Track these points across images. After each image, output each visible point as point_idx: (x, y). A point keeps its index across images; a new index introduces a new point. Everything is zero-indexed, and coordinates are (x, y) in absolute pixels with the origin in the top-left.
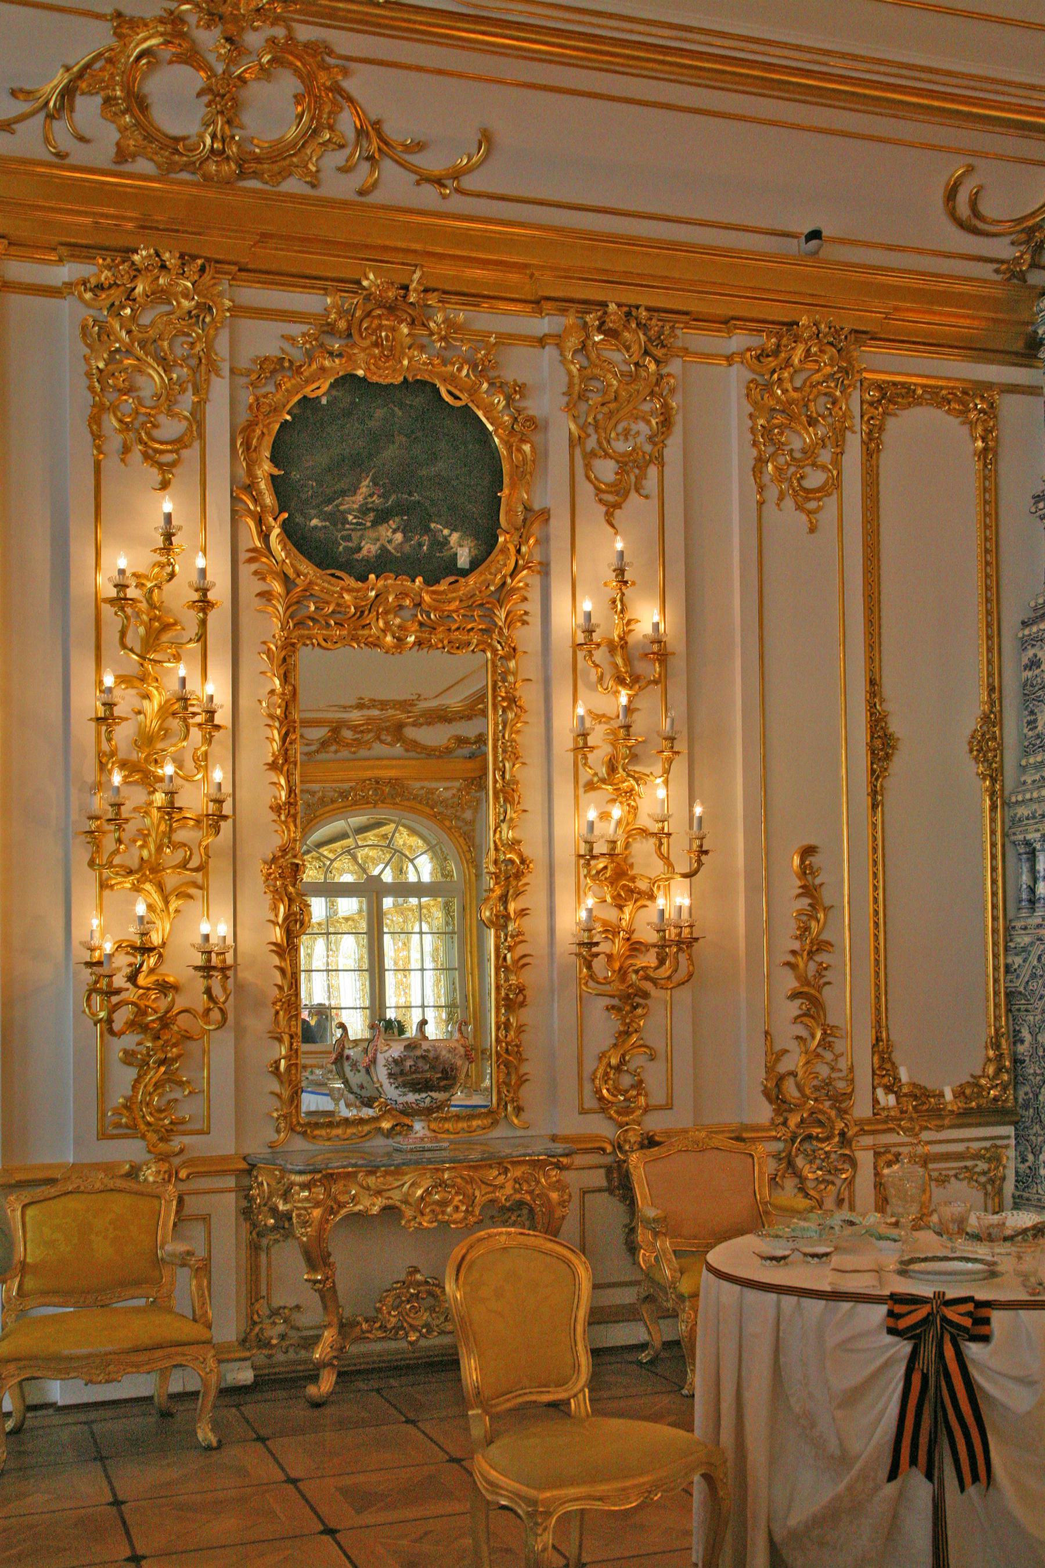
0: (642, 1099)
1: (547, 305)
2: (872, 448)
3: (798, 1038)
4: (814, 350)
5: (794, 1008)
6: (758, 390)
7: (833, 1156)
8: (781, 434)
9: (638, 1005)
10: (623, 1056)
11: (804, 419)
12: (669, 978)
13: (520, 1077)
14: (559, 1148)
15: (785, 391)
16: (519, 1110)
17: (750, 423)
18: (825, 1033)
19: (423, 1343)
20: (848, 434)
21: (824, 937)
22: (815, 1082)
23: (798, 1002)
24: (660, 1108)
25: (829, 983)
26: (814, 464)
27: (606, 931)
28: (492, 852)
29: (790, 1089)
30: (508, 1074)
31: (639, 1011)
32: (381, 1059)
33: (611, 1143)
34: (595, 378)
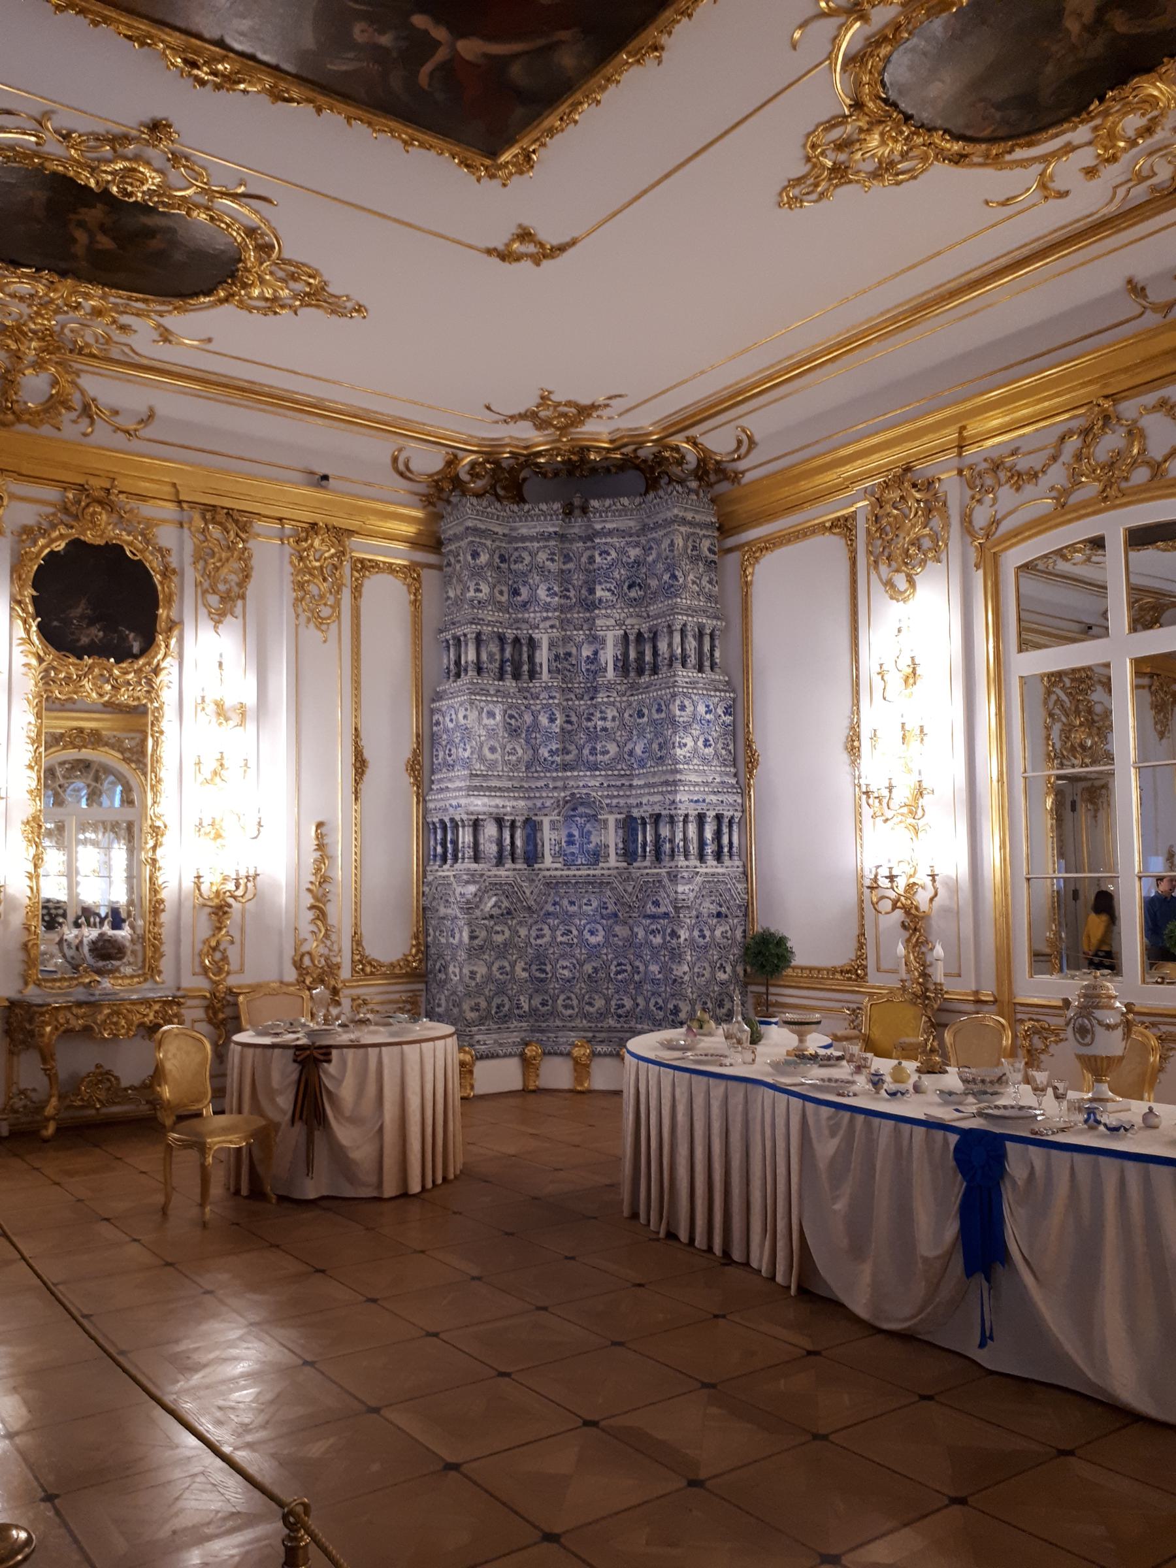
3: (313, 932)
5: (310, 915)
16: (160, 973)
18: (327, 930)
19: (104, 1110)
24: (236, 973)
26: (325, 604)
29: (307, 961)
32: (85, 941)
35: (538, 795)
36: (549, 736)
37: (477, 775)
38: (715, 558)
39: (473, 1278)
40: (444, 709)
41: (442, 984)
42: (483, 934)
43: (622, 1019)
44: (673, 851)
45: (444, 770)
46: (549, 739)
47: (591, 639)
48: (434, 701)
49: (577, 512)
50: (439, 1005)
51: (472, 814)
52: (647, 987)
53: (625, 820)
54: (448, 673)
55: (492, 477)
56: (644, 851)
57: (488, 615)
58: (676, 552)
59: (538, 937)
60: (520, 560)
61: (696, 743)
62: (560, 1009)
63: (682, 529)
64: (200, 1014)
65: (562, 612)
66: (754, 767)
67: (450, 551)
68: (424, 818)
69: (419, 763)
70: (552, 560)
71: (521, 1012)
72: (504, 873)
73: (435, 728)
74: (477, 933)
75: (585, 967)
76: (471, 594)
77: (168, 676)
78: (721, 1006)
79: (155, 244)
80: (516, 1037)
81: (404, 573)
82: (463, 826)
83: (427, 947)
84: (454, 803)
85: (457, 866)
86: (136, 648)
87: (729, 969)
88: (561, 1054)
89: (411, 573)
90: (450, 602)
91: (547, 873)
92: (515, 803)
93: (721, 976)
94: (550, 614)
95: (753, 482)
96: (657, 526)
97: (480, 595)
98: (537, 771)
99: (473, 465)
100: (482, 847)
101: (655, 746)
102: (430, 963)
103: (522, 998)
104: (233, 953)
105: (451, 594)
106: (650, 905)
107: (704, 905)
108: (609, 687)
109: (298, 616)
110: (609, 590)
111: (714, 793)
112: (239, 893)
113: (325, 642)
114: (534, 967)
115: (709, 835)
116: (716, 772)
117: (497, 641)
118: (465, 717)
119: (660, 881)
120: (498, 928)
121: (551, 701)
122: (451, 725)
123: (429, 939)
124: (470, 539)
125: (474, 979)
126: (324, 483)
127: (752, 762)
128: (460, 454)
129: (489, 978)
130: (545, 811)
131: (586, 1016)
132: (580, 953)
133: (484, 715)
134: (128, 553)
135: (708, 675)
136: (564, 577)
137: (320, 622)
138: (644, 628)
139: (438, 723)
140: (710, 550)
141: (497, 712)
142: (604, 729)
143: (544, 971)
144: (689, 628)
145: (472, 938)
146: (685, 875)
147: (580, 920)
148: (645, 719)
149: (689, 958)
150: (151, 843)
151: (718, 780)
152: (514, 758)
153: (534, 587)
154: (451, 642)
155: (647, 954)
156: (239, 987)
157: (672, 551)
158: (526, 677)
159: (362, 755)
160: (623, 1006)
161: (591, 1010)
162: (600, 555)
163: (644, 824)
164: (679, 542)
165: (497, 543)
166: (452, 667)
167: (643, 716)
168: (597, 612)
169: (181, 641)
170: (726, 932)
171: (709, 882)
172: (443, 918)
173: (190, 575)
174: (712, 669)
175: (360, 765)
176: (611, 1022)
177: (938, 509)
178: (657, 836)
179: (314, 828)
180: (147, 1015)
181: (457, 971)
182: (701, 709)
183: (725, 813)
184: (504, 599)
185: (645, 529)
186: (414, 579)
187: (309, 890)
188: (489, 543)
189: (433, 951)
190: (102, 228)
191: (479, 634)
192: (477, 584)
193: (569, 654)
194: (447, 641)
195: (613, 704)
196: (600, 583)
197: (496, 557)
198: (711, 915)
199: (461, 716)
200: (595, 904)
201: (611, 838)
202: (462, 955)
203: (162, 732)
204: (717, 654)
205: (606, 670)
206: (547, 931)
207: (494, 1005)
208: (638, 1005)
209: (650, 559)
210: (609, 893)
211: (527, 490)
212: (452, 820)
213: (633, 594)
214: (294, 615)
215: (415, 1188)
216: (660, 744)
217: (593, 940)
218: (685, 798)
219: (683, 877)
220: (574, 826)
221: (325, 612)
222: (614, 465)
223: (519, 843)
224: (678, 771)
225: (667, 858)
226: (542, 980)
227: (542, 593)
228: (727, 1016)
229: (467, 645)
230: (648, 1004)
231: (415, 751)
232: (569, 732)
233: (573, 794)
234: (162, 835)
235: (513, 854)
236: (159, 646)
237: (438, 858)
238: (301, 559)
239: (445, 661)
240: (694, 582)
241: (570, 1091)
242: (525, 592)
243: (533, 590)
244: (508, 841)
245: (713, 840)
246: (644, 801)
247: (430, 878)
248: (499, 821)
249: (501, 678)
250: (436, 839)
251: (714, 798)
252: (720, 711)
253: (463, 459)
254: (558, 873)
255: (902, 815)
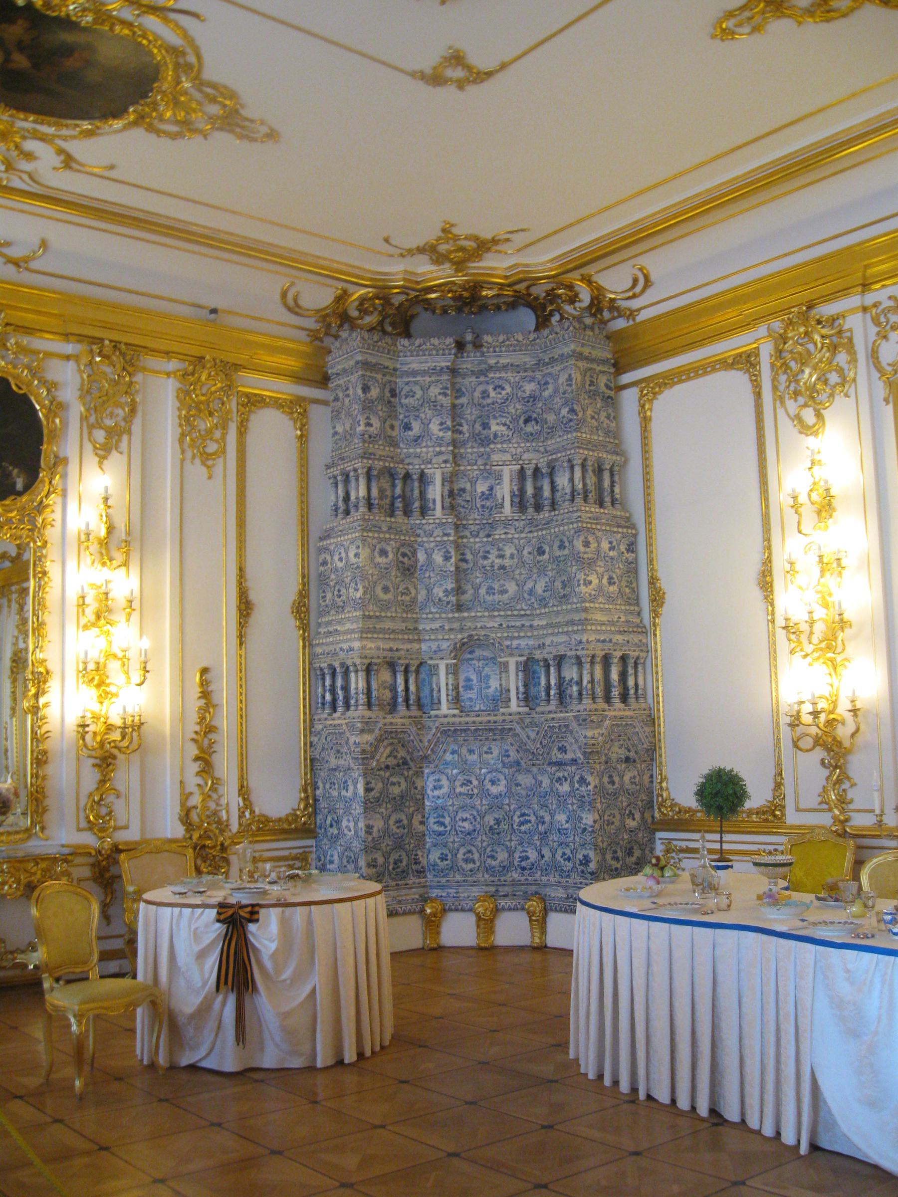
0: (112, 823)
1: (71, 337)
2: (242, 432)
3: (199, 785)
4: (213, 373)
5: (196, 767)
6: (183, 395)
7: (217, 858)
8: (194, 420)
9: (110, 764)
10: (102, 795)
11: (207, 413)
12: (127, 747)
13: (44, 808)
14: (66, 851)
15: (196, 396)
17: (178, 413)
20: (230, 423)
21: (213, 723)
22: (208, 813)
23: (199, 762)
25: (215, 752)
26: (211, 439)
27: (93, 717)
28: (30, 666)
29: (194, 817)
30: (37, 806)
31: (111, 767)
33: (95, 850)
34: (95, 381)
35: (433, 637)
36: (443, 574)
37: (370, 617)
38: (612, 393)
39: (450, 1155)
40: (332, 547)
41: (334, 839)
42: (380, 785)
43: (527, 872)
44: (580, 694)
45: (333, 612)
46: (445, 577)
47: (485, 474)
48: (321, 539)
49: (469, 347)
50: (331, 862)
51: (366, 657)
52: (554, 837)
53: (526, 663)
54: (336, 510)
55: (380, 313)
56: (548, 695)
57: (380, 449)
58: (574, 386)
59: (435, 788)
60: (411, 394)
61: (600, 581)
62: (461, 863)
63: (582, 364)
64: (86, 872)
65: (455, 447)
66: (661, 605)
67: (337, 386)
68: (310, 664)
69: (304, 606)
70: (445, 395)
71: (419, 867)
72: (400, 719)
73: (321, 568)
74: (373, 785)
75: (486, 819)
76: (361, 429)
77: (53, 514)
78: (630, 853)
79: (70, 63)
80: (414, 894)
81: (291, 408)
82: (357, 671)
83: (316, 800)
84: (345, 646)
85: (349, 714)
86: (19, 486)
87: (637, 816)
88: (463, 910)
89: (297, 409)
90: (337, 437)
91: (446, 720)
92: (409, 646)
93: (631, 824)
94: (443, 449)
95: (642, 322)
96: (553, 360)
97: (371, 429)
98: (431, 613)
99: (363, 300)
100: (374, 694)
101: (558, 584)
102: (319, 817)
103: (419, 853)
104: (119, 807)
105: (339, 429)
106: (555, 751)
107: (613, 749)
108: (507, 523)
109: (183, 452)
110: (505, 425)
111: (620, 632)
112: (125, 743)
113: (210, 478)
114: (432, 820)
115: (615, 676)
116: (621, 611)
117: (387, 475)
118: (357, 555)
119: (566, 726)
120: (394, 779)
121: (445, 538)
122: (340, 565)
123: (318, 792)
124: (360, 373)
125: (370, 834)
126: (213, 316)
127: (658, 599)
128: (351, 288)
129: (386, 832)
130: (440, 655)
131: (489, 869)
132: (481, 804)
133: (376, 554)
134: (14, 387)
135: (609, 510)
136: (455, 411)
137: (206, 458)
138: (543, 464)
139: (325, 563)
140: (607, 386)
141: (389, 549)
142: (503, 567)
143: (442, 824)
144: (590, 463)
145: (368, 790)
146: (594, 718)
147: (481, 769)
148: (546, 556)
149: (599, 805)
150: (33, 691)
151: (623, 619)
152: (408, 598)
153: (426, 422)
154: (339, 478)
155: (553, 803)
156: (126, 843)
157: (571, 385)
158: (417, 514)
159: (246, 597)
160: (528, 858)
161: (494, 863)
162: (495, 389)
163: (548, 667)
164: (577, 376)
165: (388, 378)
166: (341, 504)
167: (544, 553)
168: (492, 446)
169: (64, 476)
170: (634, 777)
171: (617, 725)
172: (335, 770)
173: (77, 409)
174: (613, 505)
175: (245, 607)
176: (515, 875)
177: (843, 345)
178: (561, 680)
179: (198, 675)
180: (35, 874)
181: (352, 825)
182: (605, 545)
183: (632, 654)
184: (394, 434)
185: (539, 364)
186: (299, 413)
187: (193, 740)
188: (379, 377)
189: (323, 804)
190: (21, 47)
191: (370, 469)
192: (368, 418)
193: (463, 490)
194: (335, 477)
195: (511, 540)
196: (495, 418)
197: (387, 390)
198: (619, 760)
199: (351, 555)
200: (496, 752)
201: (514, 682)
202: (357, 809)
203: (45, 573)
204: (617, 490)
205: (502, 506)
206: (445, 782)
207: (391, 860)
208: (543, 856)
209: (546, 394)
210: (510, 740)
211: (415, 326)
212: (343, 665)
213: (529, 428)
214: (179, 451)
215: (350, 1056)
216: (563, 582)
217: (494, 790)
218: (592, 638)
219: (592, 721)
220: (471, 669)
221: (212, 447)
222: (504, 303)
223: (412, 688)
224: (585, 610)
225: (575, 702)
226: (440, 834)
227: (434, 427)
228: (637, 864)
229: (357, 480)
230: (554, 855)
231: (301, 594)
232: (465, 570)
233: (471, 636)
234: (45, 682)
235: (407, 700)
236: (43, 481)
237: (327, 706)
238: (187, 393)
239: (333, 498)
240: (593, 418)
241: (471, 948)
242: (416, 427)
243: (426, 425)
244: (401, 688)
245: (619, 681)
246: (548, 641)
247: (319, 727)
248: (392, 666)
249: (392, 516)
250: (324, 685)
251: (619, 638)
252: (623, 548)
253: (352, 295)
254: (457, 720)
255: (821, 649)
